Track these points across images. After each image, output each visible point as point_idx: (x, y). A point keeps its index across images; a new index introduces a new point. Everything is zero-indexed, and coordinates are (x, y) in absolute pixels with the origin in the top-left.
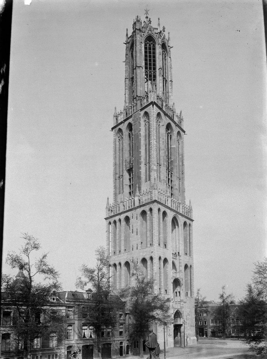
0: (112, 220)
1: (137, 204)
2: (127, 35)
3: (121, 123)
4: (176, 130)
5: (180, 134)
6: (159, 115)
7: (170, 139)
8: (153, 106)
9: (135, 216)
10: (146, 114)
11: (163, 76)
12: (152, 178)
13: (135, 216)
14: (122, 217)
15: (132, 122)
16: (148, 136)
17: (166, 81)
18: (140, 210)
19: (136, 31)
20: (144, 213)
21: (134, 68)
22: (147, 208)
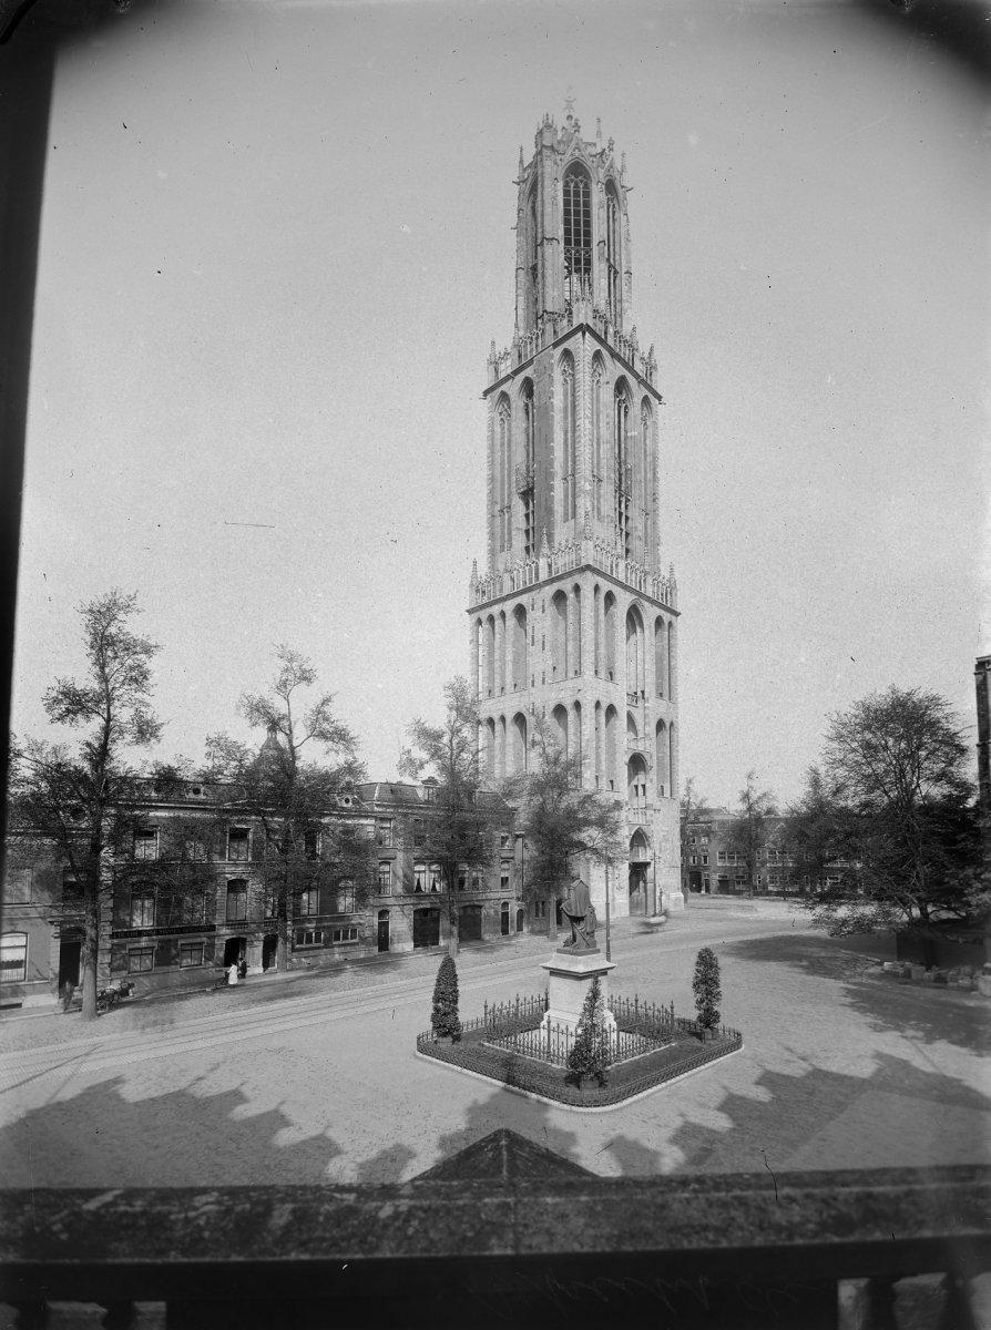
0: (484, 615)
1: (544, 576)
2: (521, 162)
3: (508, 378)
4: (638, 393)
5: (649, 403)
6: (597, 356)
7: (626, 416)
8: (584, 334)
9: (539, 604)
10: (567, 354)
11: (608, 260)
12: (581, 512)
13: (539, 604)
14: (509, 606)
15: (533, 377)
16: (572, 408)
17: (616, 272)
18: (550, 591)
19: (545, 151)
20: (560, 597)
21: (539, 241)
22: (567, 585)
